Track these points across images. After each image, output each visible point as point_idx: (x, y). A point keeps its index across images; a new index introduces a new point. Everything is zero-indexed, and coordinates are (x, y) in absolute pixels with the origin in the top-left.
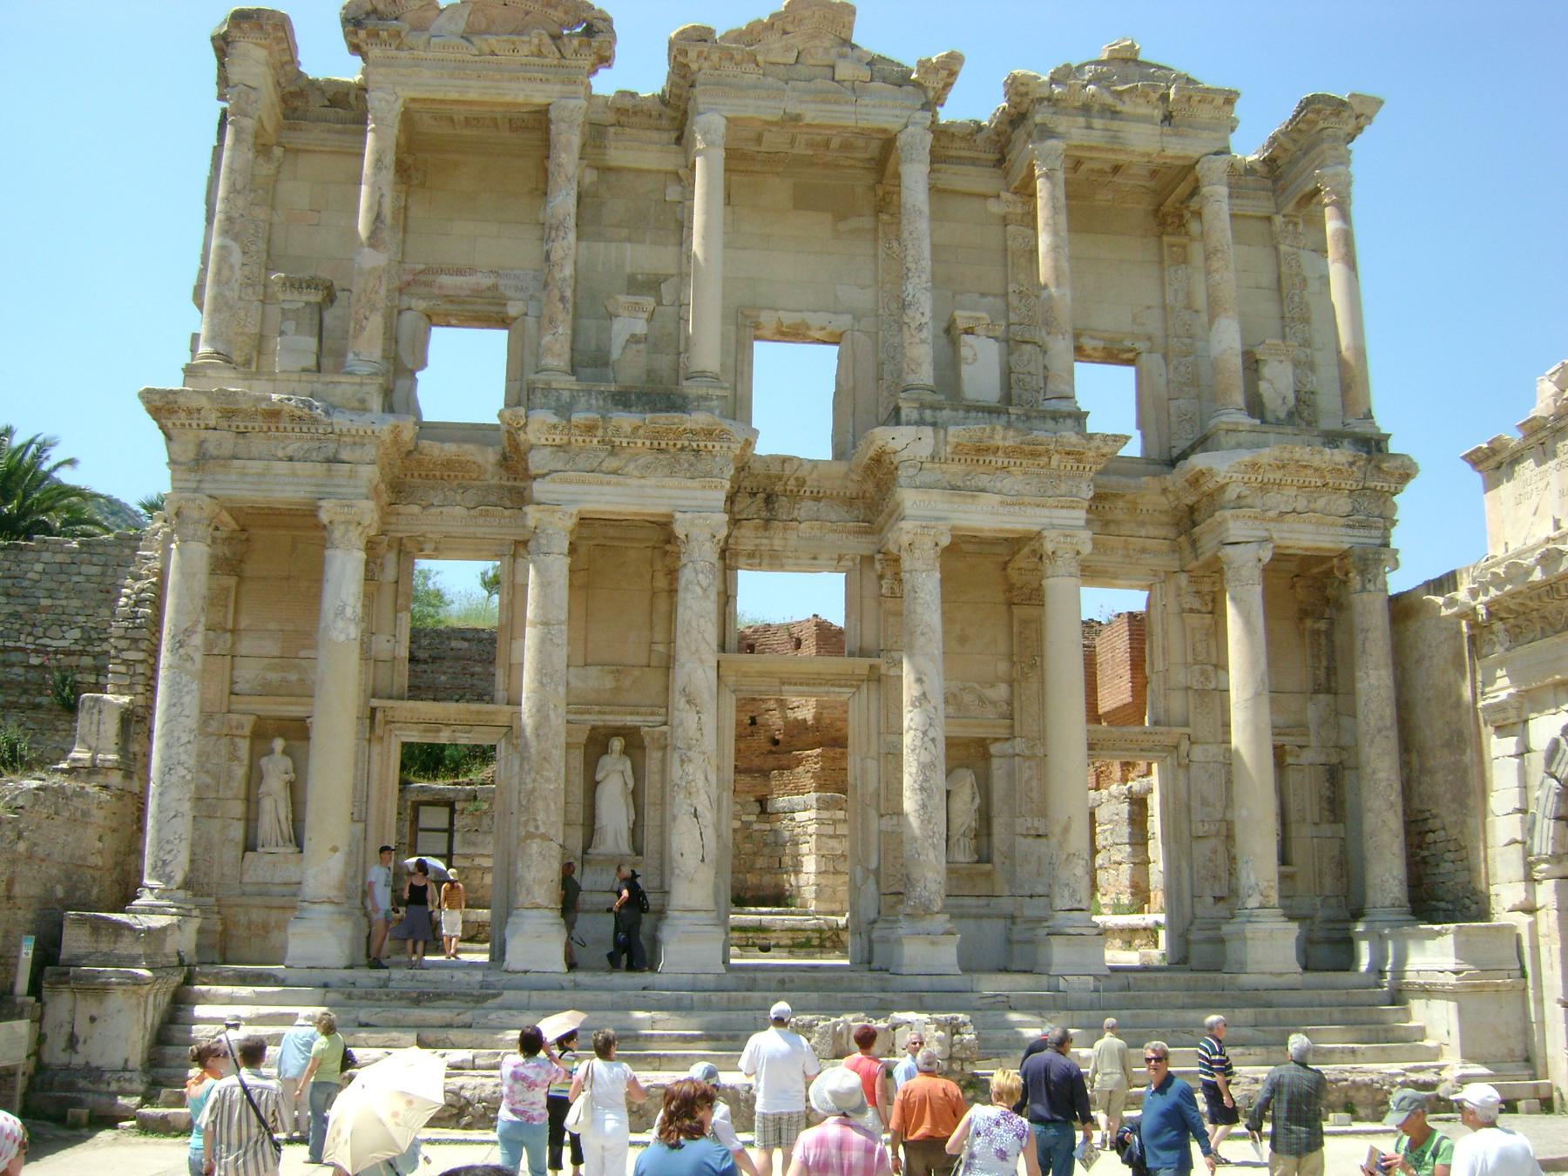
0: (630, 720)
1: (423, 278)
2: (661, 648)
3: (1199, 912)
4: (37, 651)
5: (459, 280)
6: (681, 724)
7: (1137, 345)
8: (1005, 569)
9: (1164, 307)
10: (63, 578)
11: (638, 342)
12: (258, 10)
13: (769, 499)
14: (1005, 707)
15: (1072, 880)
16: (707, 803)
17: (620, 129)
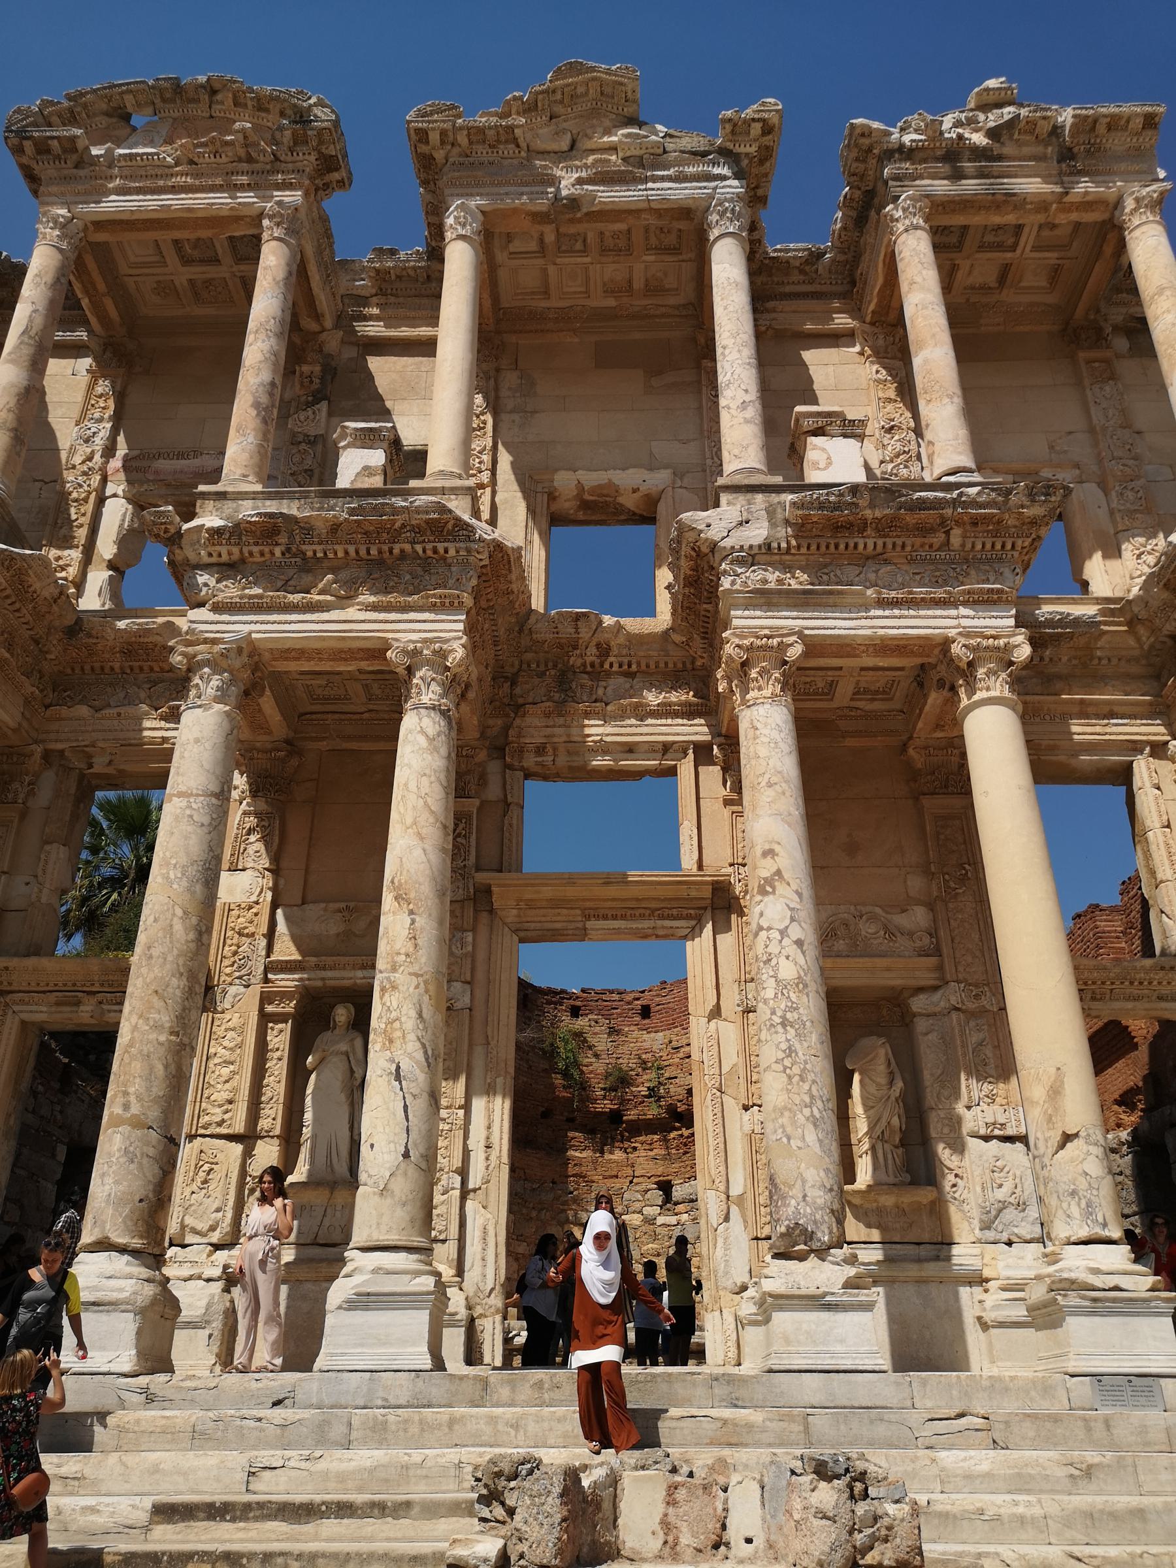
1: (134, 464)
8: (904, 747)
9: (1092, 430)
11: (371, 475)
14: (926, 940)
15: (1082, 1184)
16: (420, 1056)
17: (383, 301)
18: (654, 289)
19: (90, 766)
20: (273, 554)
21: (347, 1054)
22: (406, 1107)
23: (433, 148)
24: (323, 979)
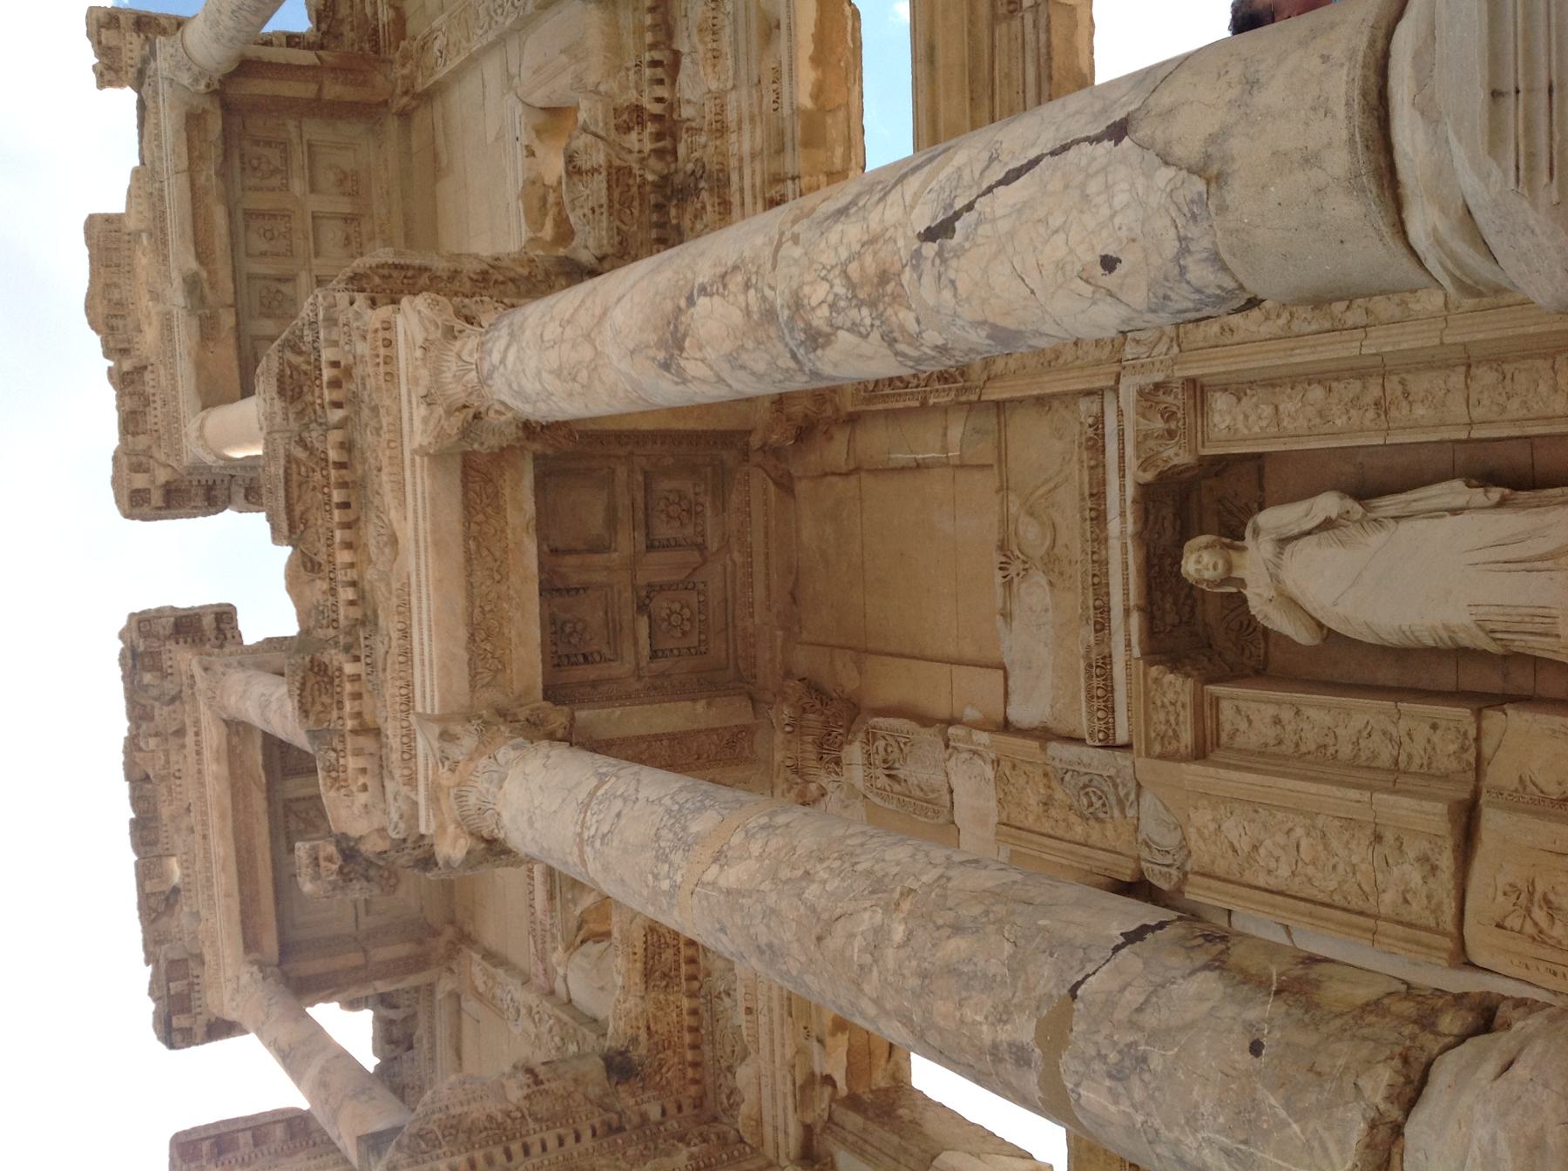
0: (1121, 525)
2: (956, 433)
6: (733, 360)
18: (351, 184)
19: (828, 1080)
20: (356, 678)
21: (1284, 542)
22: (1008, 179)
23: (153, 482)
24: (1127, 612)
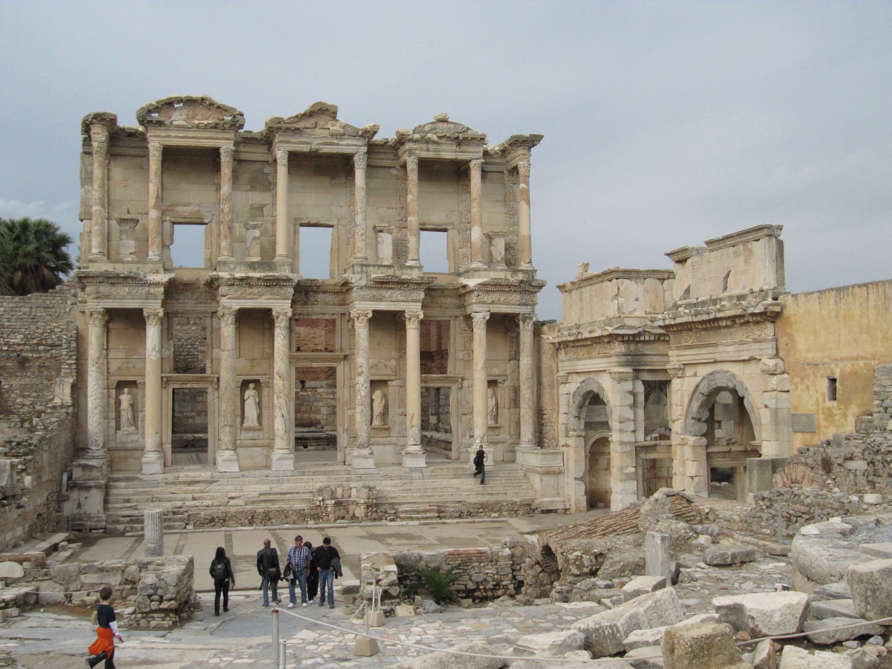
0: (256, 377)
1: (170, 208)
3: (464, 441)
4: (5, 345)
5: (185, 208)
7: (447, 227)
10: (13, 313)
12: (104, 114)
13: (306, 293)
